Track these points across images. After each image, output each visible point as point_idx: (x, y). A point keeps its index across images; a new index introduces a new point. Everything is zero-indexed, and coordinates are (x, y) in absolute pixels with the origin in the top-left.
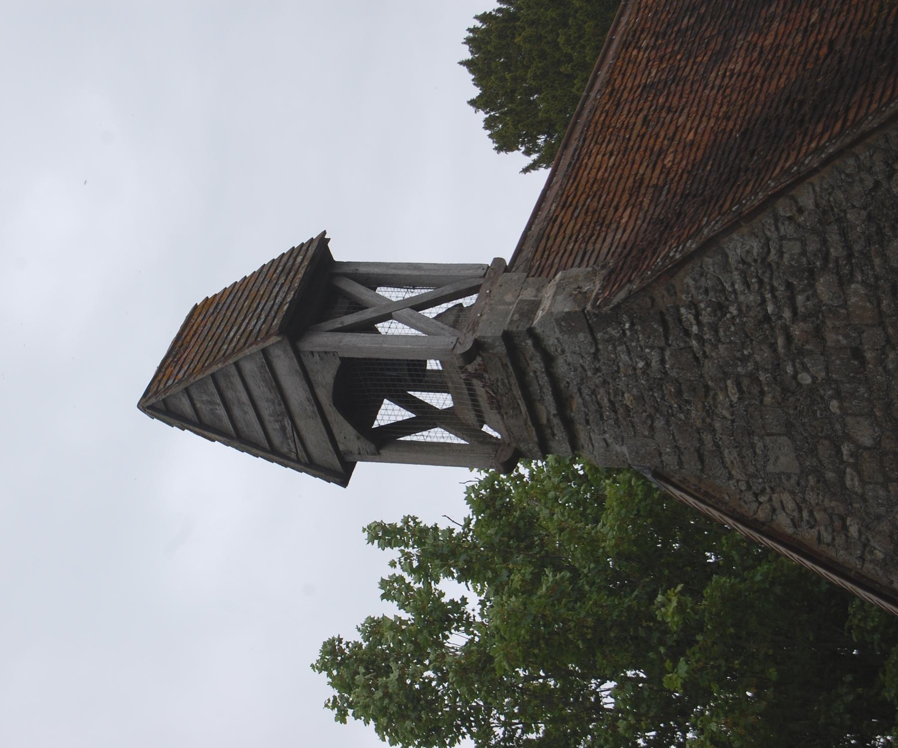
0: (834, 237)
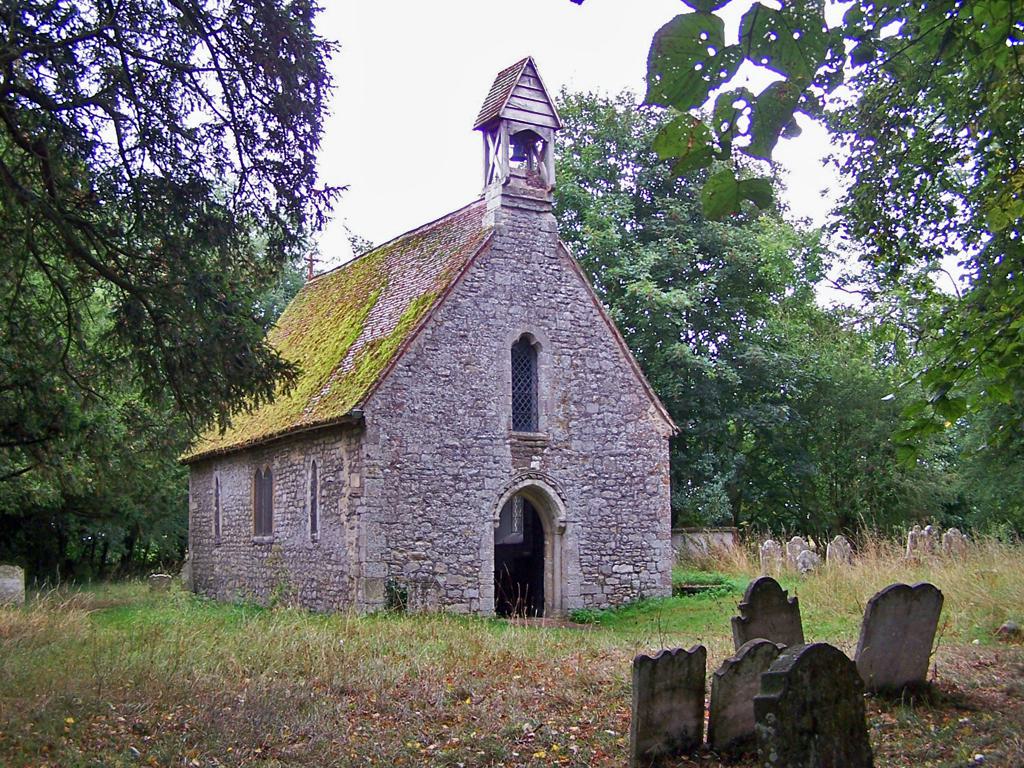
0: (585, 323)
